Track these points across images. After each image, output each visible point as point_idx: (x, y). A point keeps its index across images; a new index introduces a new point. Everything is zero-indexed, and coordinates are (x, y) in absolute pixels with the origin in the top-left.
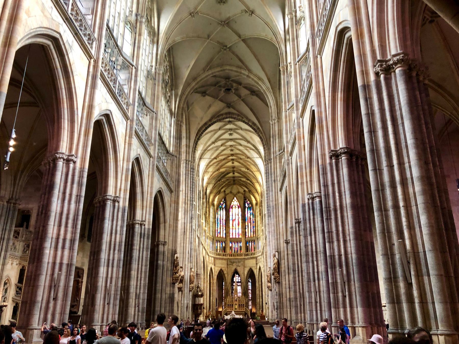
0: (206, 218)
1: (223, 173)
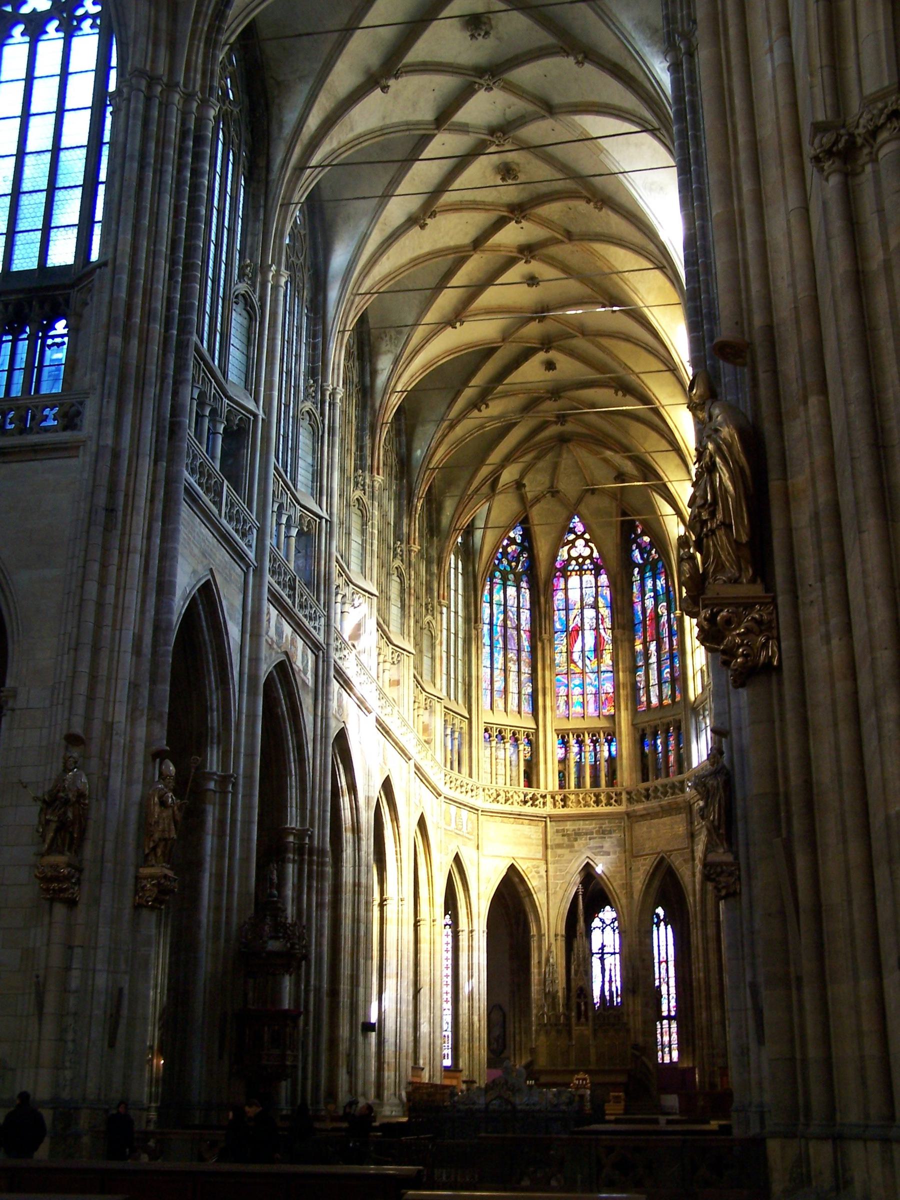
1: (486, 352)
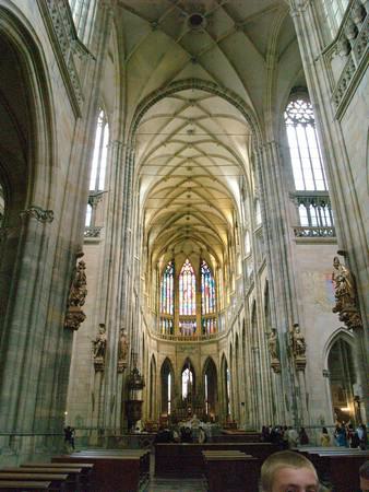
0: (146, 278)
1: (173, 214)
